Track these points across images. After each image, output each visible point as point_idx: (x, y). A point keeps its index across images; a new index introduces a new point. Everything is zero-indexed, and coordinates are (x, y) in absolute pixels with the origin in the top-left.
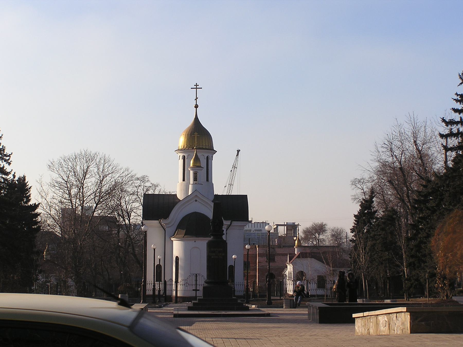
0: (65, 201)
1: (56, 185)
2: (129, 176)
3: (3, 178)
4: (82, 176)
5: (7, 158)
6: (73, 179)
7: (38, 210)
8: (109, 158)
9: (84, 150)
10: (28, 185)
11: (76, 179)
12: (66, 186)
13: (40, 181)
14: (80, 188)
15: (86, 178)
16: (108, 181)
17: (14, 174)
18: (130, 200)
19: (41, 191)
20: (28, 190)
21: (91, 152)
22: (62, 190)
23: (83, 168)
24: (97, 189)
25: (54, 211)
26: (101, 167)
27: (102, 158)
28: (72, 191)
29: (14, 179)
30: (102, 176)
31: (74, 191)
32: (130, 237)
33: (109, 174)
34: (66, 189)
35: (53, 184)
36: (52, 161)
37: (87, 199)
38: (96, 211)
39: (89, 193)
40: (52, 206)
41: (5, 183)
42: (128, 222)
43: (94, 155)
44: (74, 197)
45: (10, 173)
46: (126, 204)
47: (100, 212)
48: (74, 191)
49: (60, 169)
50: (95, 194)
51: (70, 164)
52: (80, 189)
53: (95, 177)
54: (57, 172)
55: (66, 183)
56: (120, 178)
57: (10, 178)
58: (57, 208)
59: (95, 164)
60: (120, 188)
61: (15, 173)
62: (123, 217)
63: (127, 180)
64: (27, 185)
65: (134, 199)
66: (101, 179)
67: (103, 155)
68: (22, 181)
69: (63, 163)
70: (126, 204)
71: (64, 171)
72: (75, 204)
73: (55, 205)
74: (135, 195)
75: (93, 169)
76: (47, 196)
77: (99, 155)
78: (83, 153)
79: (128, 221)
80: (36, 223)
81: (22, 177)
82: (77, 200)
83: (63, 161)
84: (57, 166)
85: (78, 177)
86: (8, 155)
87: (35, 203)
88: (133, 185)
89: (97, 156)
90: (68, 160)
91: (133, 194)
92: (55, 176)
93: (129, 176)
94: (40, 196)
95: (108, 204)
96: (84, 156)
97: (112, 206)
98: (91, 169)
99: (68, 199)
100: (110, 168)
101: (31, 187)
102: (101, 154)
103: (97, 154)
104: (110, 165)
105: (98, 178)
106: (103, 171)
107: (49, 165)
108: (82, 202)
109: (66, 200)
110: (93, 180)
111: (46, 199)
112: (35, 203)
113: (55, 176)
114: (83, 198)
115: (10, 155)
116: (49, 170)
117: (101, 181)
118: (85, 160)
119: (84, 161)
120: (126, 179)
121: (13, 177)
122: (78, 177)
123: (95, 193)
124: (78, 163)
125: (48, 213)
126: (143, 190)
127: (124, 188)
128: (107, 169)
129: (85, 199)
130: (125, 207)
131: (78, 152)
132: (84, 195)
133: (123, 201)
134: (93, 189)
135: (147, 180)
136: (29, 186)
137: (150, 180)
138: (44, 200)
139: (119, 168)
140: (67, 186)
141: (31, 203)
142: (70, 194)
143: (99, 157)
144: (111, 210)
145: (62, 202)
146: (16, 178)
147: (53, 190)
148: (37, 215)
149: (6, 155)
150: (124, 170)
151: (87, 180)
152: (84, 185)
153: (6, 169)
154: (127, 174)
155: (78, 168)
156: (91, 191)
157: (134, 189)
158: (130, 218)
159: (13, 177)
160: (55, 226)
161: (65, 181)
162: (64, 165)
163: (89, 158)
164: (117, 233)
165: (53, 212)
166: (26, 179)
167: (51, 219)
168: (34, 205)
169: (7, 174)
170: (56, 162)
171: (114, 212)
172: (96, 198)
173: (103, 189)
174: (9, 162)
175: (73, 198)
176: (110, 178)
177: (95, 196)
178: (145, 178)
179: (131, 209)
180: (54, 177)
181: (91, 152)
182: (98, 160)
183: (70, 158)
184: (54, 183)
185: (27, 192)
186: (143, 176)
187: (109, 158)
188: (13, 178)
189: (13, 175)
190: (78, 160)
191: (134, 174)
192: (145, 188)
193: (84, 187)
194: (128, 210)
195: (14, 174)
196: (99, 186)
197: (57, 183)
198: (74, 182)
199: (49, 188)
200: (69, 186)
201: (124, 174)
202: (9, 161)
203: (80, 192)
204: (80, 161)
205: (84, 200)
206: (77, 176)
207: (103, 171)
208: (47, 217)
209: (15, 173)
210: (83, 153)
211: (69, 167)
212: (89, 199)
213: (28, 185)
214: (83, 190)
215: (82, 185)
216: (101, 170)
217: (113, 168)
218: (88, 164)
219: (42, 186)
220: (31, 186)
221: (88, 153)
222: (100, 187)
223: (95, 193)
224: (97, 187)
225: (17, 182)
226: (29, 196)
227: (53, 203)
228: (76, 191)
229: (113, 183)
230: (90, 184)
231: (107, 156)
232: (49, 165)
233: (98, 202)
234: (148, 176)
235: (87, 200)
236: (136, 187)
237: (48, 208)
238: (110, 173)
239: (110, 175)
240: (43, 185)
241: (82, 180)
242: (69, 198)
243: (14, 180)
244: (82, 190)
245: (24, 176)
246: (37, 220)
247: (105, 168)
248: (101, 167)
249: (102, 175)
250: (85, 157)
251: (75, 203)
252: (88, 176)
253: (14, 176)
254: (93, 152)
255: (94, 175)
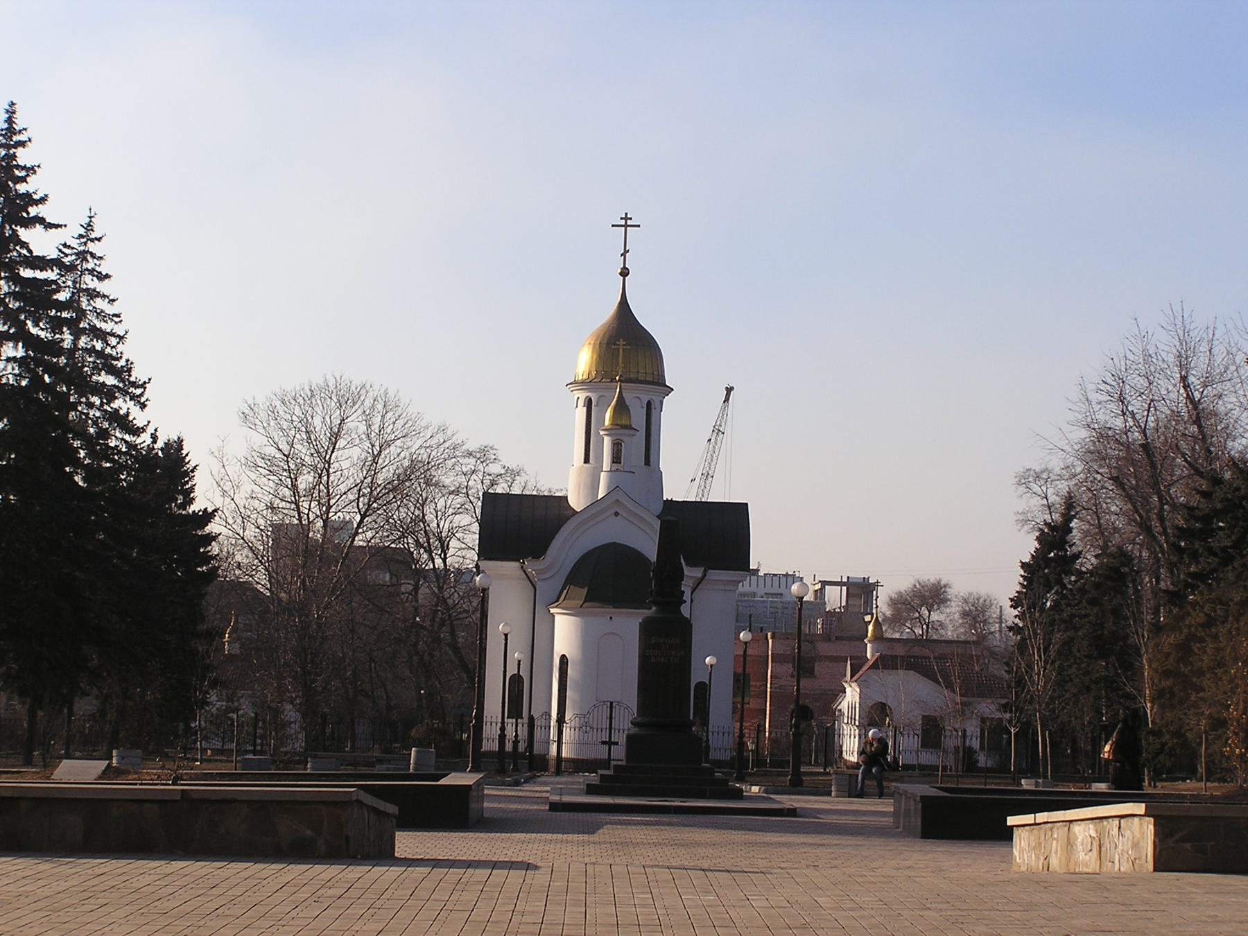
0: (283, 504)
1: (260, 462)
2: (447, 445)
3: (126, 442)
4: (327, 444)
5: (138, 391)
6: (304, 451)
7: (213, 527)
8: (397, 399)
9: (333, 375)
10: (189, 462)
11: (313, 451)
12: (286, 467)
13: (221, 453)
14: (322, 473)
15: (337, 447)
16: (392, 458)
17: (153, 432)
18: (447, 507)
19: (222, 479)
20: (189, 474)
21: (351, 382)
22: (275, 477)
23: (329, 423)
24: (365, 478)
25: (253, 530)
26: (377, 420)
27: (380, 399)
28: (299, 480)
29: (153, 446)
30: (377, 444)
31: (305, 481)
32: (445, 601)
33: (398, 439)
34: (285, 474)
35: (253, 460)
36: (250, 402)
37: (339, 503)
38: (361, 533)
39: (343, 488)
40: (249, 517)
41: (131, 456)
42: (442, 565)
43: (358, 390)
44: (304, 496)
45: (143, 430)
46: (437, 517)
47: (371, 536)
48: (305, 481)
49: (272, 423)
50: (360, 490)
51: (298, 411)
52: (320, 477)
53: (360, 445)
54: (262, 431)
55: (286, 459)
56: (422, 451)
57: (144, 442)
58: (261, 522)
59: (360, 412)
60: (423, 476)
61: (156, 430)
62: (429, 551)
63: (443, 456)
64: (187, 461)
65: (459, 506)
66: (376, 453)
67: (382, 391)
68: (175, 451)
69: (281, 409)
70: (439, 518)
71: (282, 429)
72: (308, 515)
73: (255, 516)
74: (460, 495)
75: (355, 424)
76: (237, 491)
77: (373, 390)
78: (332, 383)
79: (441, 560)
80: (207, 558)
81: (175, 442)
82: (313, 503)
83: (278, 403)
84: (263, 415)
85: (317, 445)
86: (140, 383)
87: (206, 509)
88: (457, 468)
89: (367, 392)
90: (294, 402)
91: (456, 492)
92: (259, 440)
93: (447, 445)
94: (218, 492)
95: (392, 515)
96: (332, 393)
97: (401, 522)
98: (349, 424)
99: (290, 500)
100: (400, 423)
101: (195, 467)
102: (376, 387)
103: (368, 387)
104: (399, 417)
105: (367, 448)
106: (380, 431)
107: (243, 413)
108: (324, 509)
109: (284, 503)
110: (355, 453)
111: (233, 499)
112: (206, 509)
113: (259, 440)
114: (329, 500)
115: (145, 383)
116: (244, 424)
117: (375, 461)
118: (336, 401)
119: (333, 404)
120: (439, 454)
121: (151, 440)
122: (317, 445)
123: (358, 487)
124: (319, 409)
125: (238, 534)
126: (482, 482)
127: (434, 476)
128: (391, 426)
129: (332, 502)
130: (436, 525)
131: (318, 381)
132: (331, 491)
133: (429, 509)
134: (353, 477)
135: (494, 457)
136: (193, 464)
137: (500, 458)
138: (228, 500)
139: (423, 424)
140: (289, 467)
141: (194, 508)
142: (294, 487)
143: (371, 394)
144: (400, 531)
145: (275, 508)
146: (160, 444)
147: (253, 476)
148: (211, 538)
149: (134, 385)
150: (436, 430)
151: (340, 452)
152: (332, 466)
153: (134, 419)
154: (442, 441)
155: (317, 421)
156: (350, 483)
157: (459, 480)
158: (445, 555)
159: (151, 440)
160: (254, 568)
161: (284, 455)
162: (281, 413)
163: (347, 399)
164: (412, 591)
165: (251, 532)
166: (184, 447)
167: (246, 551)
168: (203, 512)
169: (137, 431)
170: (260, 405)
171: (407, 537)
172: (361, 499)
173: (381, 479)
174: (142, 401)
175: (303, 498)
176: (399, 450)
177: (359, 494)
178: (488, 451)
179: (449, 531)
180: (255, 444)
181: (351, 382)
182: (368, 403)
183: (297, 395)
184: (256, 457)
185: (186, 479)
186: (483, 448)
187: (397, 399)
188: (152, 443)
189: (152, 434)
190: (319, 401)
191: (460, 442)
192: (487, 477)
193: (331, 471)
194: (441, 532)
195: (153, 432)
196: (369, 470)
197: (263, 459)
198: (307, 459)
199: (241, 471)
200: (292, 467)
201: (434, 442)
202: (143, 400)
203: (321, 482)
204: (323, 406)
205: (331, 504)
206: (314, 443)
207: (380, 431)
208: (235, 545)
209: (156, 430)
210: (332, 383)
211: (295, 418)
212: (343, 502)
213: (189, 462)
214: (328, 478)
215: (327, 465)
216: (376, 428)
217: (405, 424)
218: (344, 411)
219: (224, 466)
220: (197, 466)
221: (343, 384)
222: (373, 473)
223: (358, 487)
224: (365, 472)
225: (160, 454)
226: (192, 489)
227: (252, 509)
228: (311, 479)
229: (406, 463)
230: (345, 465)
231: (391, 394)
232: (243, 413)
233: (367, 510)
234: (494, 447)
235: (338, 505)
236: (465, 475)
237: (239, 520)
238: (399, 436)
239: (398, 443)
240: (228, 463)
241: (326, 453)
242: (293, 499)
243: (153, 449)
244: (325, 478)
245: (179, 438)
246: (210, 551)
247: (387, 424)
248: (377, 420)
249: (378, 441)
250: (335, 393)
251: (306, 511)
252: (341, 443)
253: (154, 438)
254: (357, 382)
255: (357, 441)
